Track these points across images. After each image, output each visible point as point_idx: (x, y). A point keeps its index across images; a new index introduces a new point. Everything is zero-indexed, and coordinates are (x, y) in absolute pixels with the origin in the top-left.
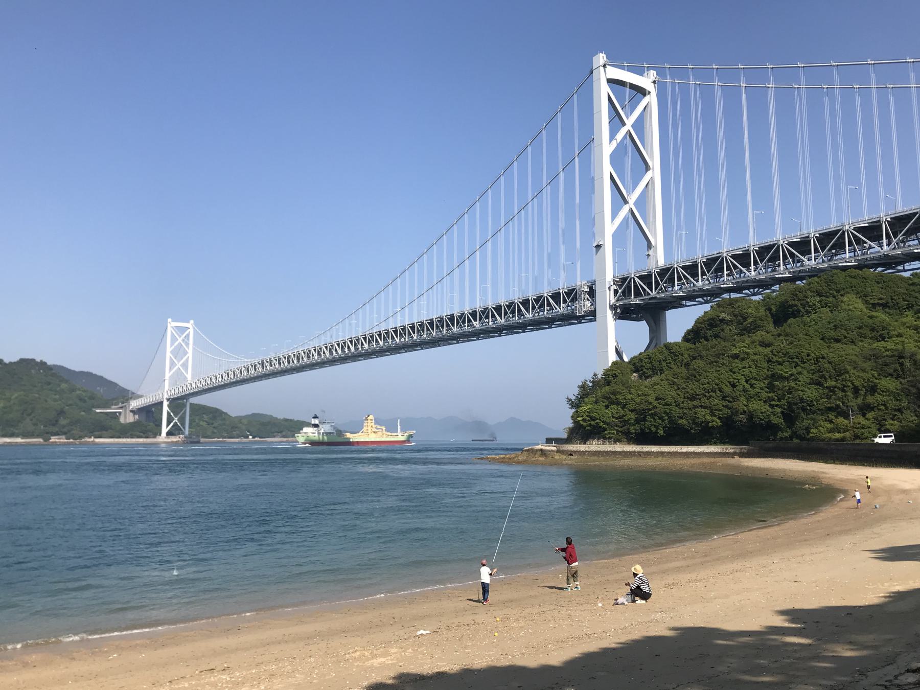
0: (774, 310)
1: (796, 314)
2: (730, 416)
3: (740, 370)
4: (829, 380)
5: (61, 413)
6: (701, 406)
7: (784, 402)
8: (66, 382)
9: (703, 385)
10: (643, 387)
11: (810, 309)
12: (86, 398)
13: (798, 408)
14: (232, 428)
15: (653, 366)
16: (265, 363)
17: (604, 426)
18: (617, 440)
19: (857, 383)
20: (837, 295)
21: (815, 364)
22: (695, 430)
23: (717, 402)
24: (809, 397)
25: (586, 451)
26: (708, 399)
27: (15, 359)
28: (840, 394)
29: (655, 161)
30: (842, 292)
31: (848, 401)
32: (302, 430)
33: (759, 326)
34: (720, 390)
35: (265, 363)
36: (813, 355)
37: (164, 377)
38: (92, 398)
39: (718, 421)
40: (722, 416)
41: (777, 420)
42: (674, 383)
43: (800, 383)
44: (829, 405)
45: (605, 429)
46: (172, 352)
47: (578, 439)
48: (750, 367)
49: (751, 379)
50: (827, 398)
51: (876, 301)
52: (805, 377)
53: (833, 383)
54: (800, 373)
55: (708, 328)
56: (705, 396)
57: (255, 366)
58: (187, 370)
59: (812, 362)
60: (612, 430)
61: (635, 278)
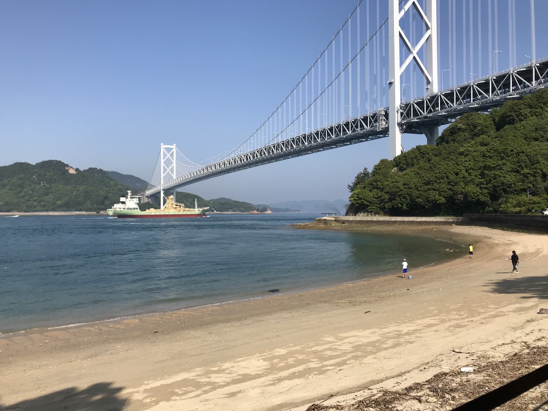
0: (497, 120)
1: (512, 122)
2: (452, 196)
3: (462, 163)
4: (525, 169)
6: (433, 189)
8: (114, 180)
9: (435, 174)
10: (397, 176)
11: (521, 117)
12: (123, 190)
13: (500, 190)
15: (407, 162)
16: (208, 168)
17: (367, 203)
18: (377, 213)
20: (544, 107)
21: (517, 157)
22: (428, 206)
23: (445, 187)
24: (508, 181)
25: (353, 221)
26: (438, 184)
27: (87, 168)
28: (532, 179)
31: (538, 184)
32: (114, 206)
33: (485, 132)
34: (447, 177)
35: (208, 168)
36: (515, 150)
37: (161, 177)
39: (444, 199)
40: (446, 196)
42: (418, 173)
43: (503, 172)
44: (522, 187)
46: (164, 163)
48: (470, 161)
49: (469, 169)
50: (523, 182)
52: (509, 166)
54: (504, 164)
55: (450, 134)
56: (437, 182)
57: (204, 170)
58: (172, 172)
59: (515, 156)
60: (373, 206)
61: (414, 104)
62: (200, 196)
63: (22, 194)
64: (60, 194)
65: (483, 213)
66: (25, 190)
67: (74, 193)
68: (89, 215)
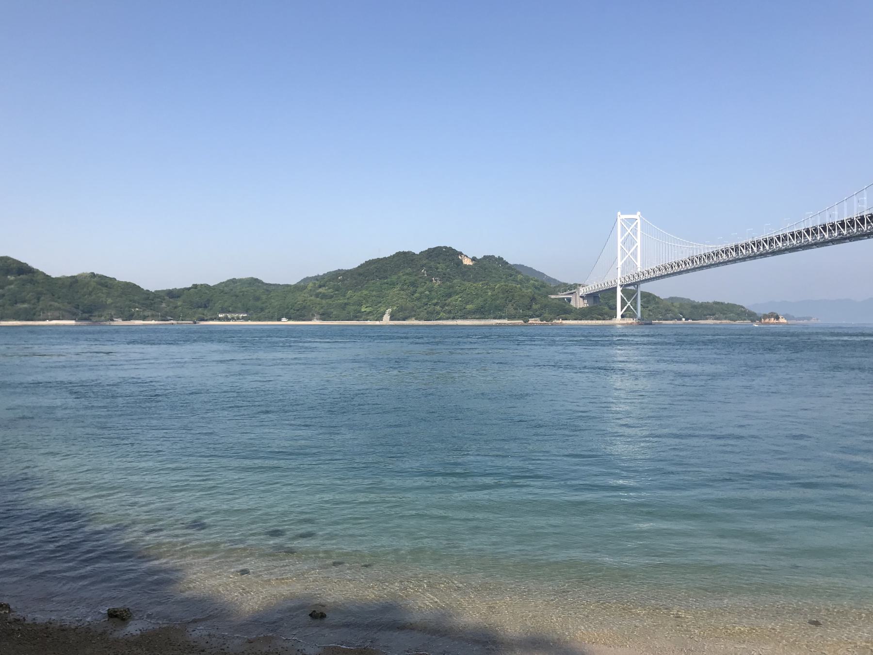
5: (533, 299)
14: (666, 311)
38: (543, 286)
62: (657, 295)
63: (417, 295)
64: (469, 294)
66: (420, 290)
67: (490, 294)
68: (514, 325)
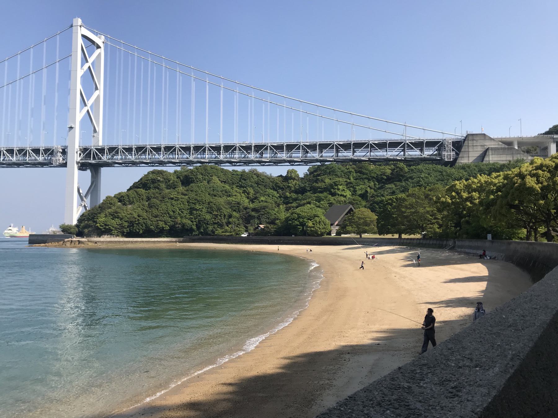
1: (193, 182)
2: (174, 225)
7: (197, 220)
15: (130, 200)
18: (118, 236)
19: (226, 214)
25: (104, 241)
28: (220, 218)
29: (101, 86)
30: (210, 175)
41: (194, 227)
42: (143, 208)
45: (112, 230)
47: (95, 235)
51: (223, 180)
52: (204, 210)
53: (217, 213)
54: (203, 208)
56: (162, 216)
65: (191, 236)
